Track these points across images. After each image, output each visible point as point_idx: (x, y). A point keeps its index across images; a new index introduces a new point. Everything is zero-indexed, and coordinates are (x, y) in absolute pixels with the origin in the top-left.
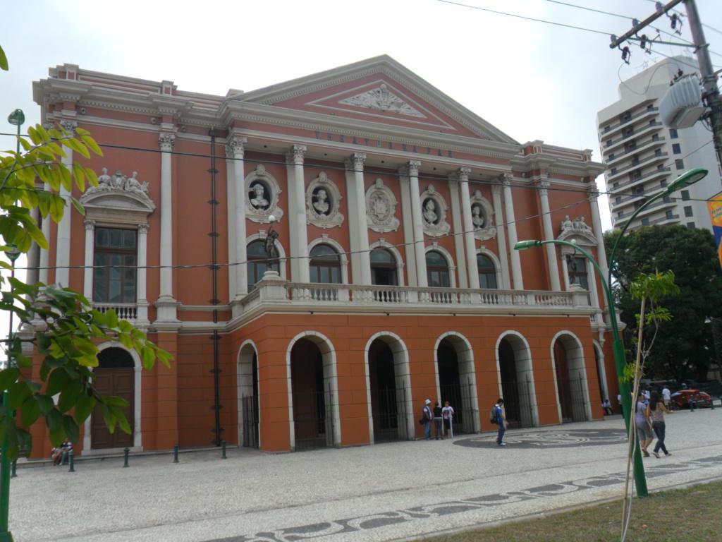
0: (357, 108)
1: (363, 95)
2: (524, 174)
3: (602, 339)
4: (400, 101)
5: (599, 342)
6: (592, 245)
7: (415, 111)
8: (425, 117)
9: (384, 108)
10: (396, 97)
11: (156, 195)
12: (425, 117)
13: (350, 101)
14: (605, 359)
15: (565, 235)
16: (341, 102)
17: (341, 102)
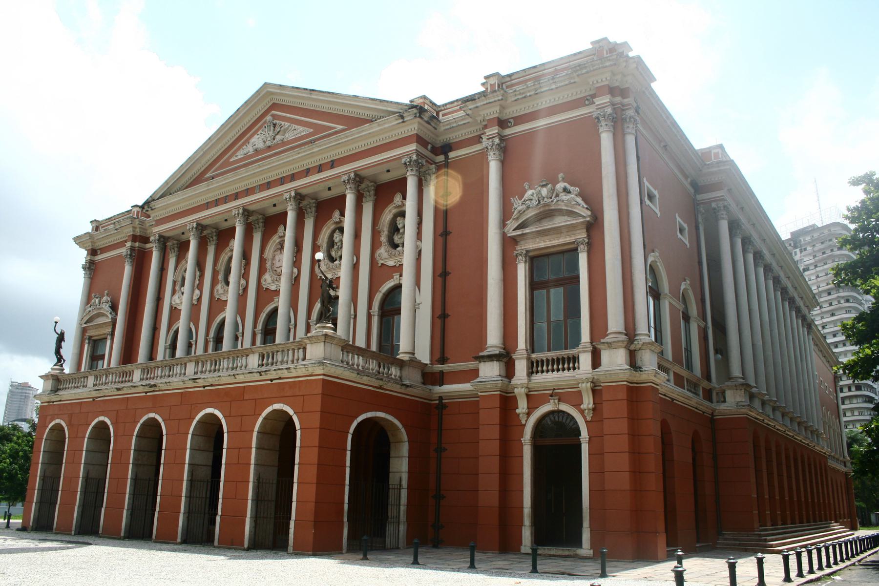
0: (247, 157)
1: (252, 140)
2: (429, 147)
3: (588, 402)
4: (287, 124)
5: (582, 412)
6: (581, 220)
7: (301, 128)
8: (311, 130)
9: (268, 143)
10: (283, 123)
11: (114, 308)
12: (311, 130)
13: (240, 155)
14: (590, 442)
15: (517, 219)
16: (232, 160)
17: (232, 160)
